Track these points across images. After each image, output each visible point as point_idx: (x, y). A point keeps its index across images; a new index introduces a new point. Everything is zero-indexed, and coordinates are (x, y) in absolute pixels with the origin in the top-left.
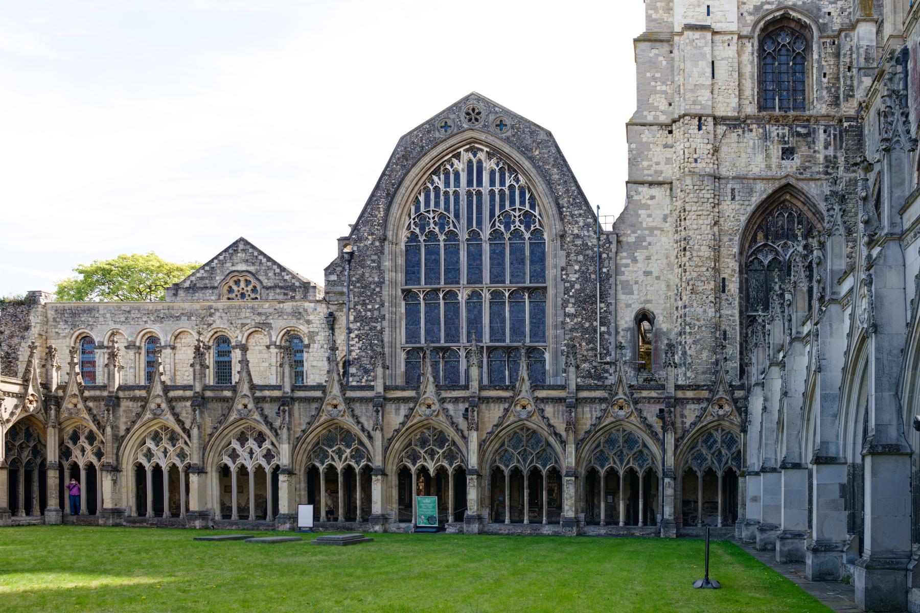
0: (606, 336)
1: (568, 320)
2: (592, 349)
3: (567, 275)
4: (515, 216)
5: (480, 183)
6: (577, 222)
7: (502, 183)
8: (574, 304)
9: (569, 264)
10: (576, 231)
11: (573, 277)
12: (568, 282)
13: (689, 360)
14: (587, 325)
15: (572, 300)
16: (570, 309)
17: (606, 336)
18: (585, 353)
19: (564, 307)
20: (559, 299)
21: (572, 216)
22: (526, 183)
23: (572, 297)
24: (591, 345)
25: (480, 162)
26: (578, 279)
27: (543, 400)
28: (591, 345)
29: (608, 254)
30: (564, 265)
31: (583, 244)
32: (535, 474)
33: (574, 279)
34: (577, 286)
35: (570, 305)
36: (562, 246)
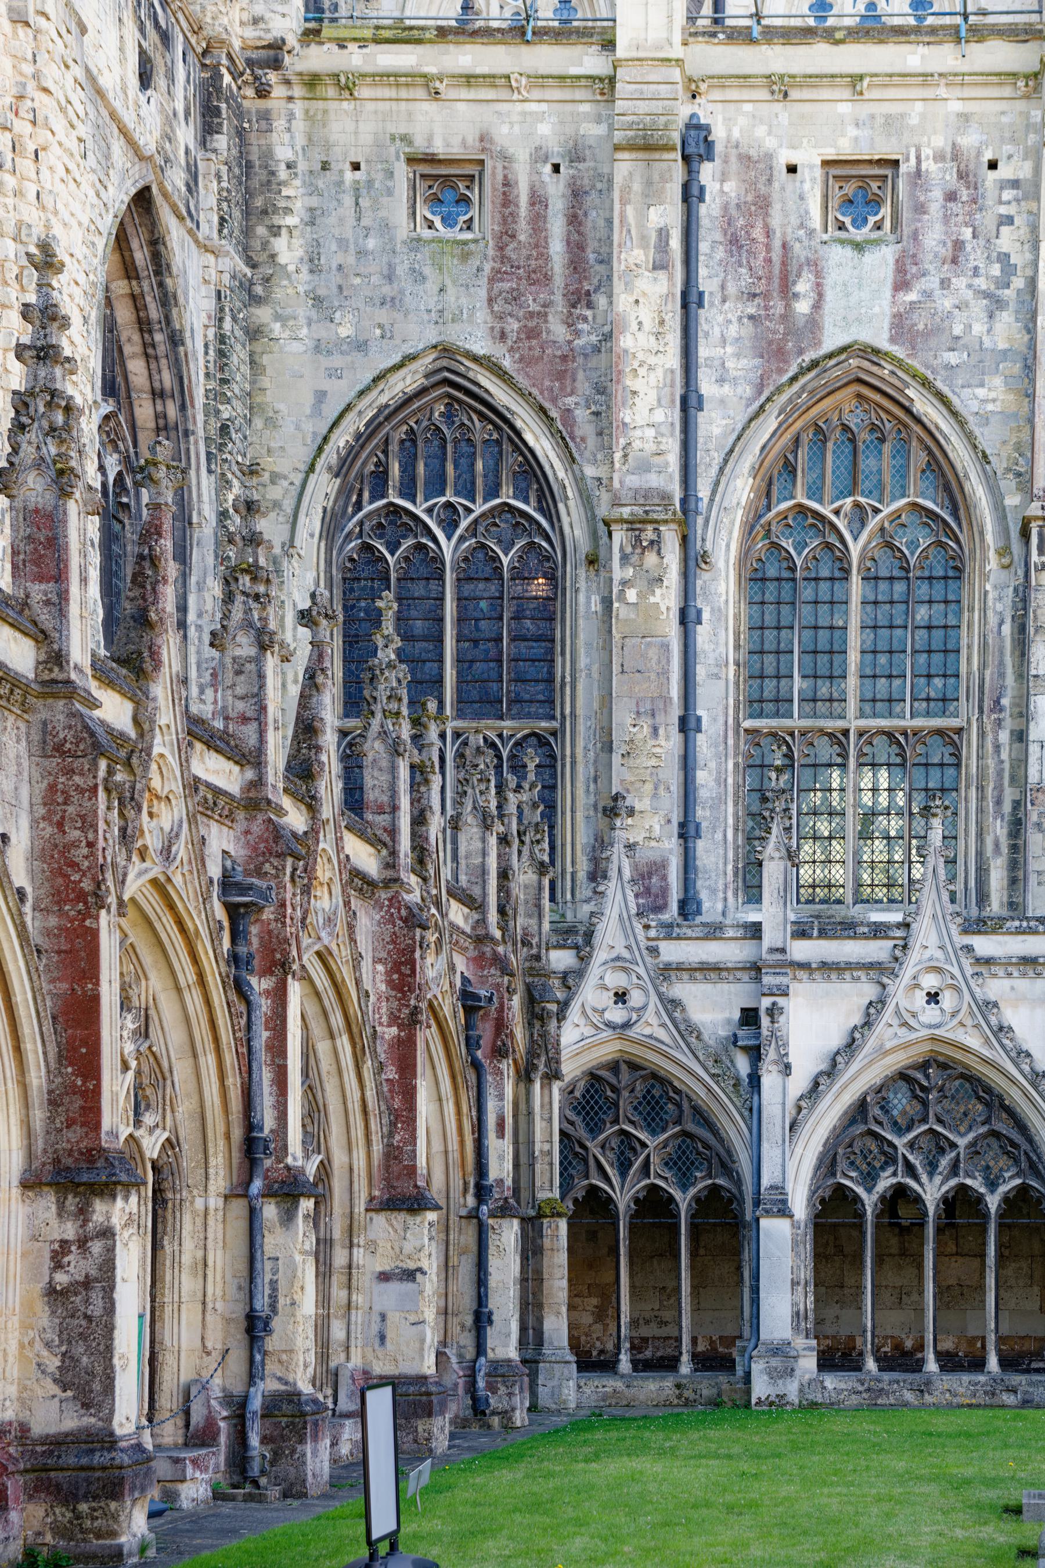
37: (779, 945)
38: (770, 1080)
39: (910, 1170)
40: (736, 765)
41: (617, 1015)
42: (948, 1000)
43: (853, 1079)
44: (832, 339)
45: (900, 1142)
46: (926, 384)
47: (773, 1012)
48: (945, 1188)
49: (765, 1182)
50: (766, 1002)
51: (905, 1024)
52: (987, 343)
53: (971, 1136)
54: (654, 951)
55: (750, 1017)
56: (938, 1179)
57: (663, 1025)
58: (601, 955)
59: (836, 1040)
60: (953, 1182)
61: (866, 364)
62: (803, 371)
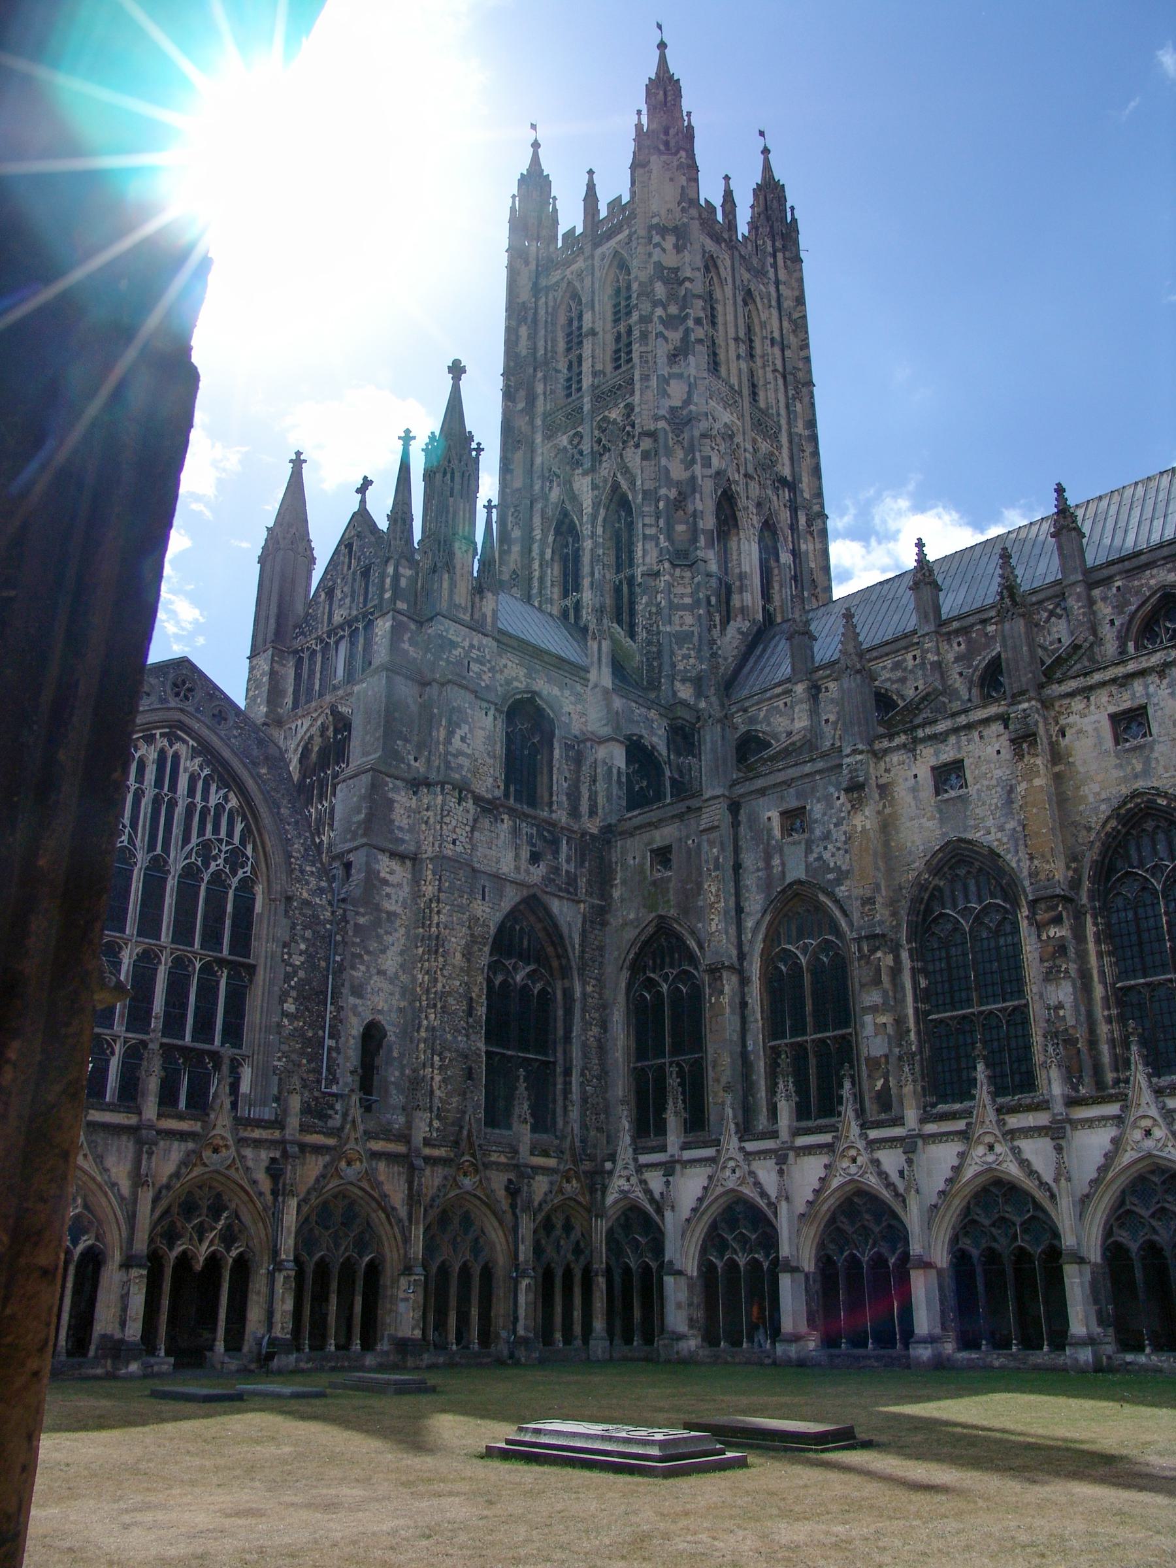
0: (334, 1055)
1: (286, 1022)
2: (314, 1071)
3: (290, 955)
4: (220, 851)
5: (173, 787)
6: (308, 883)
7: (205, 798)
8: (295, 999)
9: (293, 939)
10: (305, 895)
11: (297, 960)
12: (291, 965)
13: (437, 1103)
14: (310, 1034)
15: (294, 994)
16: (290, 1007)
17: (334, 1055)
18: (305, 1076)
19: (282, 1001)
20: (276, 988)
21: (302, 871)
22: (241, 806)
23: (293, 988)
24: (313, 1065)
25: (176, 756)
26: (303, 963)
27: (375, 1155)
28: (313, 1065)
29: (343, 937)
30: (287, 939)
31: (313, 915)
32: (348, 1267)
33: (298, 963)
34: (301, 974)
35: (290, 1000)
36: (286, 912)
41: (626, 1188)
58: (620, 1164)
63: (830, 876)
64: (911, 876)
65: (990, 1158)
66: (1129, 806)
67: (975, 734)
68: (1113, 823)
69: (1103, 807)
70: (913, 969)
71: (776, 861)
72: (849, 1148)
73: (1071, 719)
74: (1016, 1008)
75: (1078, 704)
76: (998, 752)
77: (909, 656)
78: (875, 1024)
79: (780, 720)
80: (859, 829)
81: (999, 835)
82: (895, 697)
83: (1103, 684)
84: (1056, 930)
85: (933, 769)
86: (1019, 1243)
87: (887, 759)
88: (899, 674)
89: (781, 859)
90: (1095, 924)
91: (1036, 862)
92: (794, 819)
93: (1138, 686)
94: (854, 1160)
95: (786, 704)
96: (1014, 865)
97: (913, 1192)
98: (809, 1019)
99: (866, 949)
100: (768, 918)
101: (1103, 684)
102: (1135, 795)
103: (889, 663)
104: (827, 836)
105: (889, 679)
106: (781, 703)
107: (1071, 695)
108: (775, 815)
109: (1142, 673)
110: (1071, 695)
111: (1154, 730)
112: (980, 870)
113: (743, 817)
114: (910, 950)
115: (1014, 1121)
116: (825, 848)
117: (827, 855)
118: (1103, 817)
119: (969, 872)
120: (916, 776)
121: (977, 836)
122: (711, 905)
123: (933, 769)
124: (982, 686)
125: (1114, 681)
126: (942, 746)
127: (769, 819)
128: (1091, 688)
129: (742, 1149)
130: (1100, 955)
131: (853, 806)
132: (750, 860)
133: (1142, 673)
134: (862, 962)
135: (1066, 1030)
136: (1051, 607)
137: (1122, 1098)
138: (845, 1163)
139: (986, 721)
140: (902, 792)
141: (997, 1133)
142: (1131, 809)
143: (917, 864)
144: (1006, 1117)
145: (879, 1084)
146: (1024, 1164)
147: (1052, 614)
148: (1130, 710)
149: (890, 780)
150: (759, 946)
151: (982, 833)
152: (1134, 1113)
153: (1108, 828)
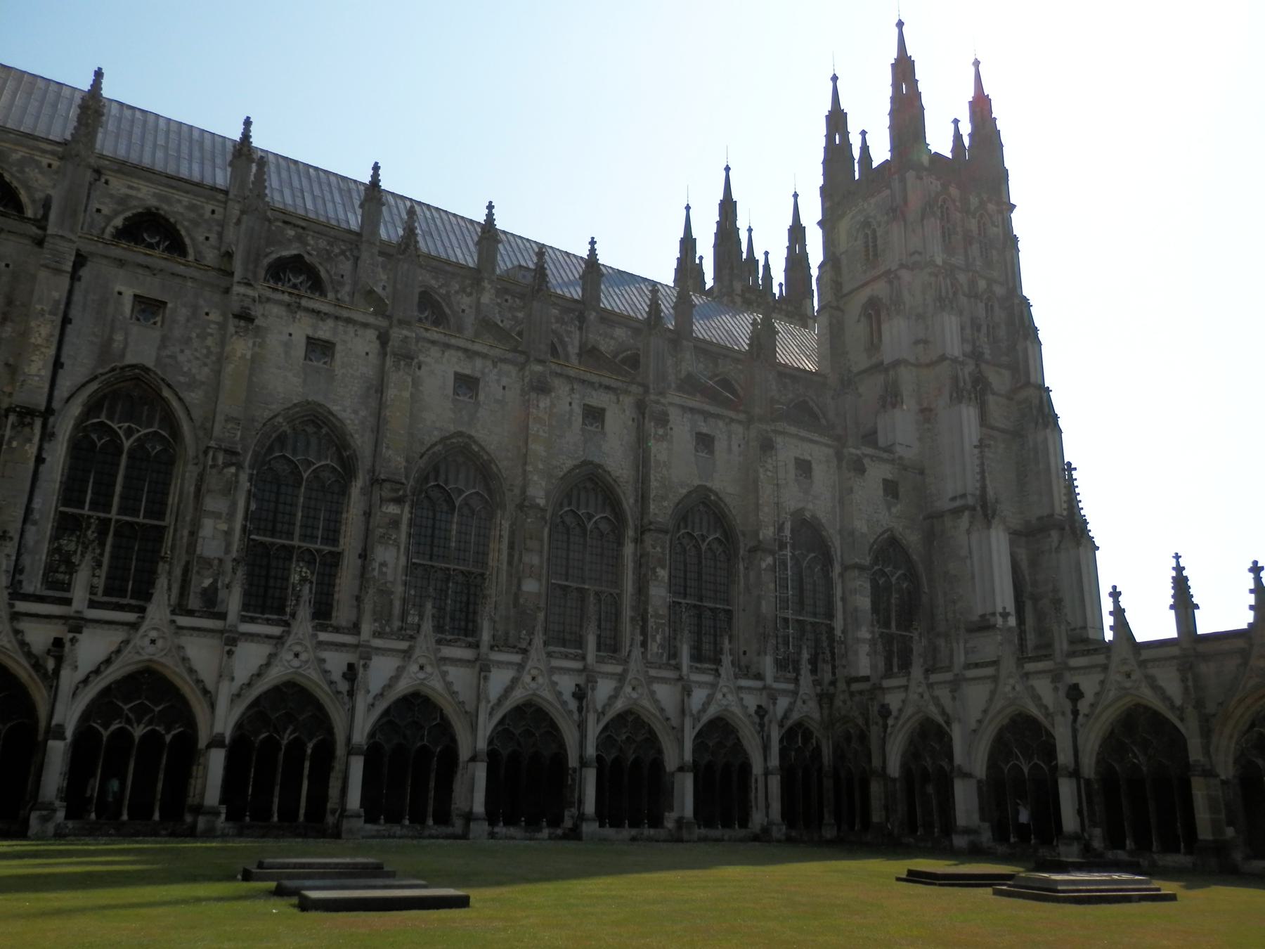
37: (80, 609)
38: (65, 673)
39: (129, 721)
40: (53, 526)
42: (160, 643)
43: (106, 677)
44: (130, 359)
45: (126, 707)
46: (169, 386)
47: (73, 641)
48: (145, 731)
49: (54, 723)
50: (71, 635)
51: (138, 653)
52: (198, 377)
53: (160, 708)
54: (12, 606)
55: (58, 643)
56: (142, 726)
57: (10, 642)
59: (102, 657)
60: (149, 728)
61: (143, 373)
62: (113, 370)
63: (182, 379)
64: (267, 414)
65: (421, 675)
66: (454, 440)
67: (351, 329)
68: (439, 447)
69: (436, 433)
70: (249, 491)
71: (119, 337)
72: (297, 643)
73: (428, 360)
74: (330, 553)
75: (435, 351)
76: (367, 354)
77: (209, 208)
78: (215, 528)
79: (39, 176)
80: (239, 354)
81: (353, 416)
82: (183, 233)
83: (458, 348)
84: (395, 507)
85: (308, 338)
86: (425, 742)
87: (268, 306)
88: (193, 215)
89: (126, 339)
90: (411, 513)
91: (390, 452)
92: (148, 307)
93: (479, 363)
94: (297, 655)
95: (50, 166)
96: (359, 442)
97: (363, 692)
98: (116, 500)
99: (220, 461)
100: (94, 386)
101: (458, 348)
102: (460, 434)
103: (186, 199)
104: (188, 341)
105: (182, 214)
106: (44, 161)
107: (433, 343)
108: (129, 293)
109: (485, 356)
110: (433, 343)
111: (482, 397)
112: (327, 434)
113: (84, 272)
114: (251, 476)
115: (447, 651)
116: (182, 351)
117: (181, 358)
118: (434, 439)
119: (315, 433)
120: (290, 335)
121: (335, 409)
122: (37, 347)
123: (308, 338)
124: (267, 271)
125: (466, 350)
126: (321, 323)
127: (120, 293)
128: (448, 346)
129: (173, 622)
130: (409, 535)
131: (236, 332)
132: (82, 321)
133: (485, 356)
134: (214, 471)
135: (386, 583)
136: (343, 247)
137: (524, 651)
138: (290, 656)
139: (366, 325)
140: (274, 341)
141: (433, 658)
142: (452, 443)
143: (274, 407)
144: (441, 647)
145: (207, 582)
146: (448, 685)
147: (343, 253)
148: (467, 376)
149: (264, 325)
150: (76, 409)
151: (339, 408)
152: (530, 664)
153: (436, 449)
